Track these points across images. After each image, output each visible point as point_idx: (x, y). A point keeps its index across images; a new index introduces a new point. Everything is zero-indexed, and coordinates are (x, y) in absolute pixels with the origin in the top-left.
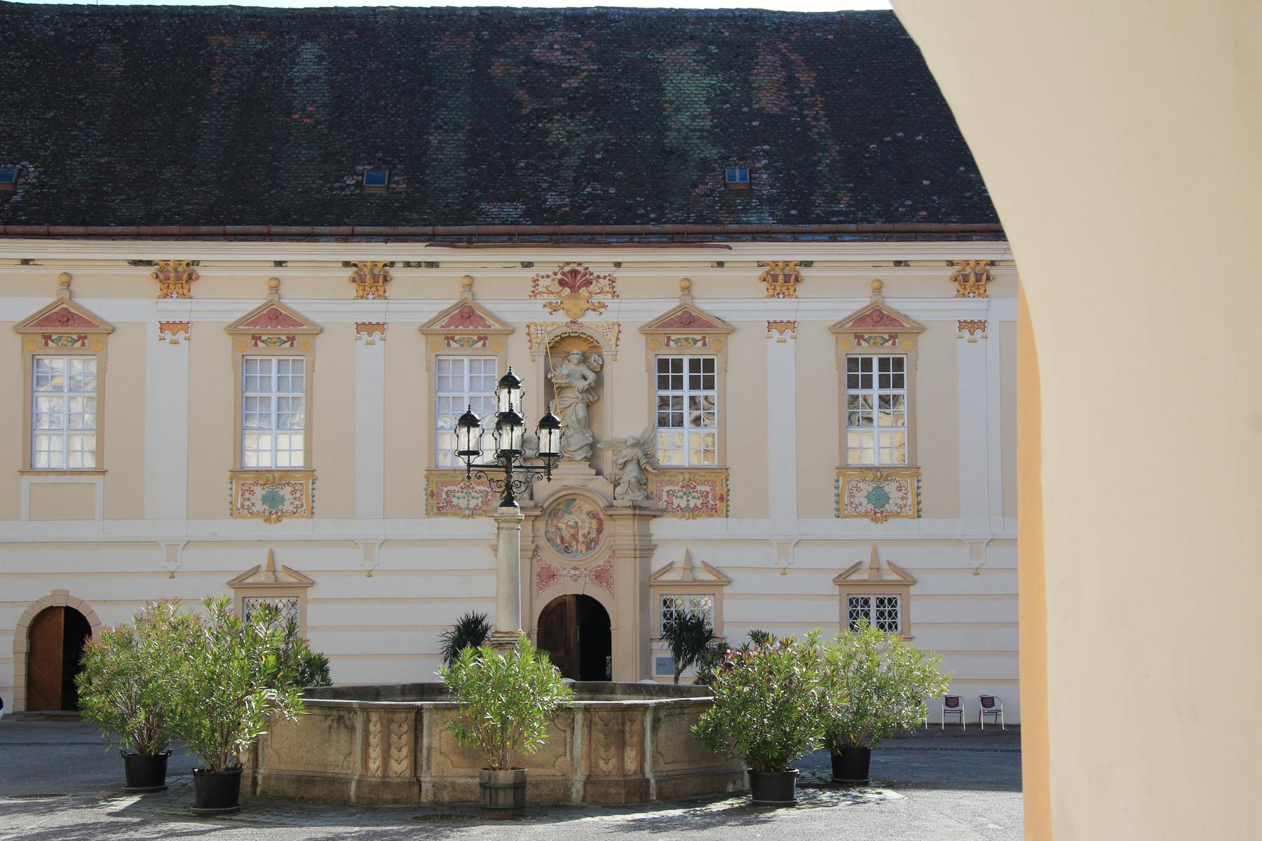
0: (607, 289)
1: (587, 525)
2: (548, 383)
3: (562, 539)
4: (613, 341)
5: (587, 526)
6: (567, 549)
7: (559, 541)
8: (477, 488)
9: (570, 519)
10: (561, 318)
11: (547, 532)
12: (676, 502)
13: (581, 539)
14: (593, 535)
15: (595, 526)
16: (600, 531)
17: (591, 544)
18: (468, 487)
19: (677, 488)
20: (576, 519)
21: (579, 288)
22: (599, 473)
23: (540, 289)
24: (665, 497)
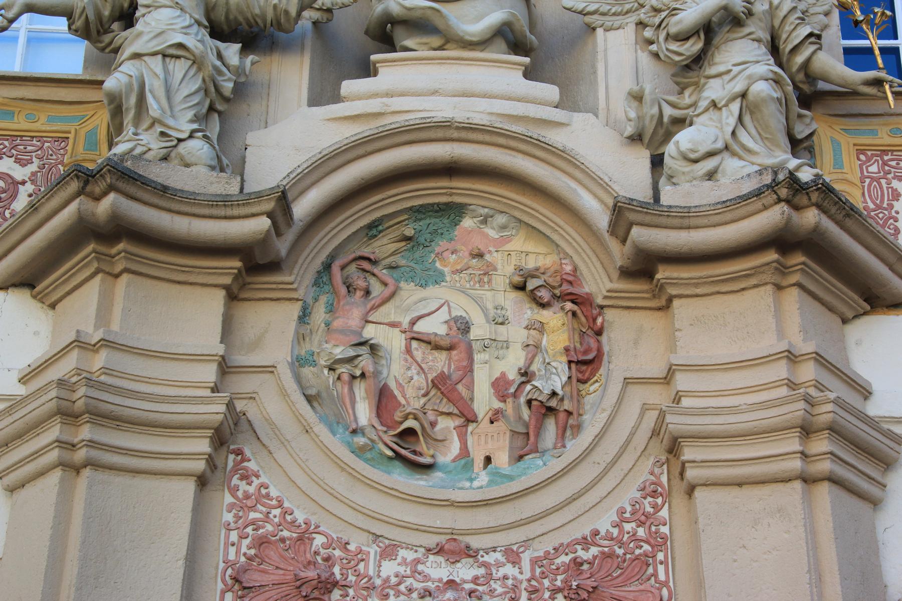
1: (516, 333)
3: (383, 400)
5: (516, 343)
6: (407, 448)
7: (364, 413)
9: (432, 305)
11: (299, 362)
13: (483, 400)
14: (554, 378)
16: (585, 364)
20: (462, 306)
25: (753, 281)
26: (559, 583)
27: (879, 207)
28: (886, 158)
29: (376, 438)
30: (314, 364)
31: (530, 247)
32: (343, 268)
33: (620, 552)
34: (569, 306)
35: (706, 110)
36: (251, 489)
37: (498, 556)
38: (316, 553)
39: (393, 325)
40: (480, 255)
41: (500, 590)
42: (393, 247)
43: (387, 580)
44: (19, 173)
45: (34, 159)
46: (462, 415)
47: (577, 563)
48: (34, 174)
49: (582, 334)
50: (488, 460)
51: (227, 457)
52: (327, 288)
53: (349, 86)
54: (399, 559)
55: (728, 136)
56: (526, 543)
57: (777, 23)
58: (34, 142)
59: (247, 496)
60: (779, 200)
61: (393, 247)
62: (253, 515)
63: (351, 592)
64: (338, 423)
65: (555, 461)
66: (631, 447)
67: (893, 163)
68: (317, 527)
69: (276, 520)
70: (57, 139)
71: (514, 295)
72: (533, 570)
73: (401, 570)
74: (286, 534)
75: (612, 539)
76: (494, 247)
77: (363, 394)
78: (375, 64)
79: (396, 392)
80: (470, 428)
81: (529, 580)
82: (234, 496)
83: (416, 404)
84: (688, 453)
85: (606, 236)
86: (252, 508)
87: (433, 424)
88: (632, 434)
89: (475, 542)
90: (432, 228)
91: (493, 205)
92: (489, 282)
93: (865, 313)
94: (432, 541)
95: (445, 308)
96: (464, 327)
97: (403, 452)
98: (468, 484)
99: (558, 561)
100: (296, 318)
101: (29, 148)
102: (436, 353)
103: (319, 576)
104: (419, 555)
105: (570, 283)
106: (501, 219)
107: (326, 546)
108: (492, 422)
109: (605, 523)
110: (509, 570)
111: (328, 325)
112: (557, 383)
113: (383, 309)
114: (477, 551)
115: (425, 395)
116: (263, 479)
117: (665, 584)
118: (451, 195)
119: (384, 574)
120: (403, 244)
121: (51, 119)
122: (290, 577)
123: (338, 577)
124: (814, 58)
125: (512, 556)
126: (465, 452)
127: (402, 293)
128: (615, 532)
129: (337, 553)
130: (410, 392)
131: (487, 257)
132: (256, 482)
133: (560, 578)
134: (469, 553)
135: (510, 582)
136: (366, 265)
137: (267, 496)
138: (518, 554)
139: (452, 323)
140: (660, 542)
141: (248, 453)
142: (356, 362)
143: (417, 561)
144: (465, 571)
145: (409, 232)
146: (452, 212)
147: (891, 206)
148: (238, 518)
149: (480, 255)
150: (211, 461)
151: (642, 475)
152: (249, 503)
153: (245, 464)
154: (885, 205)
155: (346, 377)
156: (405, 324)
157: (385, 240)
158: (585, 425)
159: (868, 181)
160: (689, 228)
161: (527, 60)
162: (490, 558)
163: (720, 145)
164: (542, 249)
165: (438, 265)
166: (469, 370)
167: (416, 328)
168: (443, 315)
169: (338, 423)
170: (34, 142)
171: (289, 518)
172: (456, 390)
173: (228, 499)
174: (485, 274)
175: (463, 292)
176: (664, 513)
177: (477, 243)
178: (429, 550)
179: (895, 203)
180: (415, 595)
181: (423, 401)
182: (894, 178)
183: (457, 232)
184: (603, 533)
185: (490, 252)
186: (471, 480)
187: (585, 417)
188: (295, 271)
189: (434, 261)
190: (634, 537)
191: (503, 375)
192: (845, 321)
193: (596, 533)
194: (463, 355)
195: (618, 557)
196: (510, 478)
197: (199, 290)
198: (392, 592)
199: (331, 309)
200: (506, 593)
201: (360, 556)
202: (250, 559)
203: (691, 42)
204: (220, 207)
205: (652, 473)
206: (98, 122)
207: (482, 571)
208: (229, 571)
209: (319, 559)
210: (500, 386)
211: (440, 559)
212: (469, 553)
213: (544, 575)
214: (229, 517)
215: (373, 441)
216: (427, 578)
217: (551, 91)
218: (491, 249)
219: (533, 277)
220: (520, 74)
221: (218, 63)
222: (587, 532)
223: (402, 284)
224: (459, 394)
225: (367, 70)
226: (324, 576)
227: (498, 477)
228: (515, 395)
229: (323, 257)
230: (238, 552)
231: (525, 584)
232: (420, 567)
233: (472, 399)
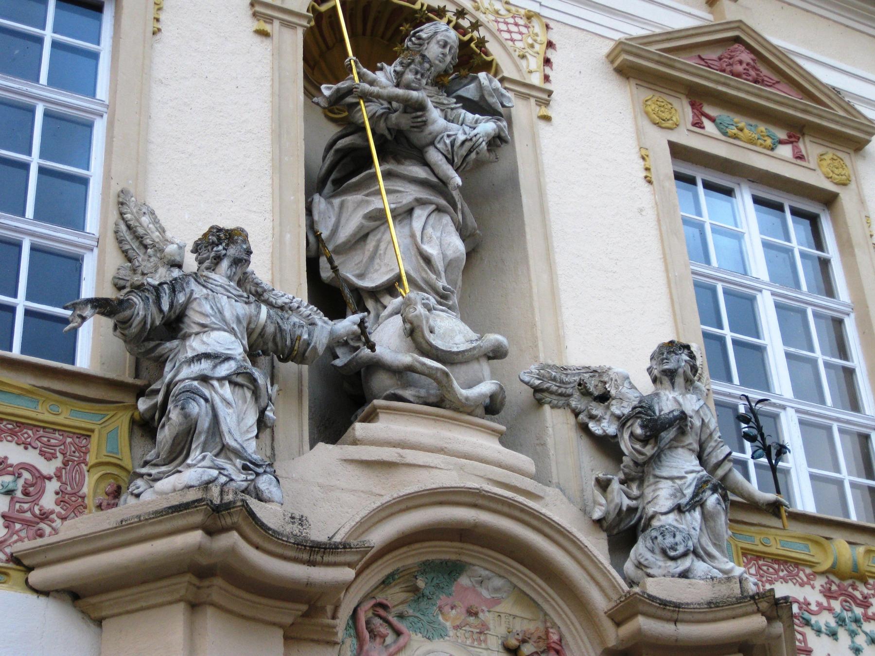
28: (761, 562)
31: (517, 611)
32: (366, 612)
40: (476, 614)
44: (48, 468)
45: (58, 454)
48: (59, 470)
53: (359, 428)
57: (703, 438)
60: (759, 611)
61: (403, 596)
67: (765, 568)
91: (497, 570)
92: (485, 641)
101: (53, 441)
106: (498, 582)
131: (481, 615)
136: (382, 612)
146: (452, 570)
149: (476, 614)
157: (397, 589)
174: (480, 633)
177: (471, 600)
185: (483, 611)
218: (484, 608)
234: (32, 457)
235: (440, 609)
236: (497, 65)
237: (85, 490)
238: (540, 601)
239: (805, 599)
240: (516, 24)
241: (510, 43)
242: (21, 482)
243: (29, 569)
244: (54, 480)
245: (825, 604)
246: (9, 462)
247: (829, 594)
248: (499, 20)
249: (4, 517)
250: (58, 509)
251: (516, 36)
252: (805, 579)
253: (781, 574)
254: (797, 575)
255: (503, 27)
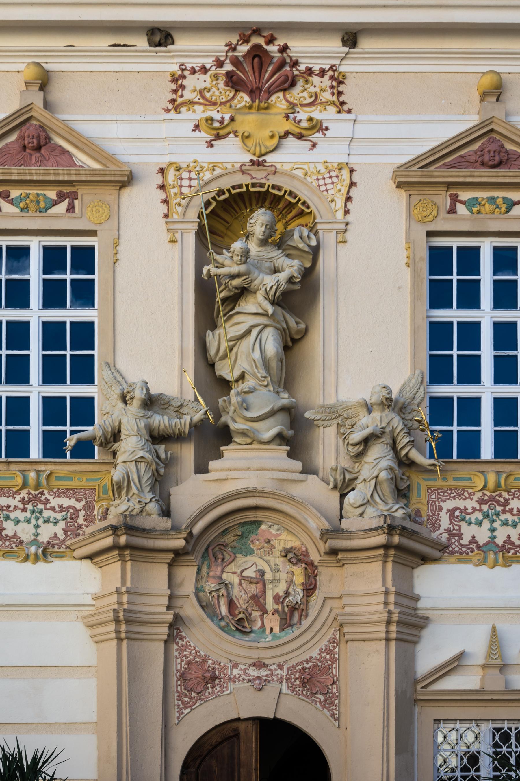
0: (327, 96)
1: (283, 576)
2: (205, 289)
3: (231, 604)
4: (340, 202)
5: (283, 580)
6: (241, 626)
8: (55, 502)
9: (249, 564)
10: (231, 153)
11: (198, 591)
12: (468, 532)
15: (299, 578)
16: (310, 589)
17: (291, 614)
18: (35, 499)
19: (470, 504)
20: (262, 565)
21: (270, 93)
22: (308, 470)
23: (188, 95)
24: (445, 522)
25: (375, 559)
26: (297, 676)
27: (434, 515)
28: (439, 491)
29: (229, 621)
30: (204, 591)
31: (289, 538)
32: (213, 550)
33: (320, 664)
34: (304, 565)
35: (362, 482)
36: (184, 643)
37: (275, 667)
38: (209, 667)
39: (234, 573)
41: (276, 679)
42: (233, 539)
43: (235, 676)
44: (79, 506)
45: (83, 499)
46: (261, 611)
47: (304, 669)
48: (84, 506)
49: (309, 577)
50: (271, 629)
51: (174, 631)
52: (207, 558)
53: (213, 464)
54: (239, 668)
55: (369, 497)
56: (286, 662)
58: (82, 491)
59: (183, 646)
62: (185, 653)
63: (222, 680)
64: (214, 616)
65: (297, 631)
66: (326, 624)
67: (442, 494)
68: (209, 657)
69: (194, 655)
70: (91, 489)
71: (282, 559)
72: (288, 672)
73: (240, 672)
74: (198, 660)
75: (317, 660)
76: (274, 537)
77: (223, 602)
78: (222, 451)
79: (236, 602)
80: (265, 615)
81: (286, 676)
82: (178, 645)
83: (244, 607)
84: (346, 629)
85: (319, 540)
86: (185, 650)
87: (250, 615)
88: (326, 620)
89: (267, 662)
90: (248, 530)
93: (422, 564)
94: (251, 661)
95: (254, 565)
96: (262, 573)
97: (240, 627)
98: (264, 640)
99: (297, 668)
100: (195, 573)
101: (81, 494)
102: (251, 585)
103: (211, 675)
104: (246, 667)
105: (304, 555)
106: (277, 527)
107: (213, 664)
108: (273, 615)
109: (314, 653)
110: (279, 672)
111: (208, 574)
112: (298, 598)
113: (229, 566)
114: (268, 665)
115: (248, 602)
116: (188, 639)
117: (336, 675)
118: (256, 517)
119: (234, 674)
120: (237, 537)
121: (88, 480)
122: (200, 676)
123: (217, 675)
124: (410, 452)
125: (280, 667)
126: (263, 625)
127: (237, 559)
128: (318, 657)
129: (217, 666)
130: (241, 602)
131: (271, 542)
132: (185, 640)
133: (297, 674)
134: (265, 665)
135: (279, 676)
136: (222, 547)
137: (190, 645)
138: (282, 666)
139: (257, 572)
140: (334, 660)
141: (181, 630)
142: (220, 590)
143: (246, 669)
144: (263, 673)
145: (239, 533)
147: (439, 514)
148: (180, 654)
149: (269, 542)
150: (169, 635)
151: (330, 635)
152: (183, 648)
153: (181, 633)
154: (436, 514)
155: (216, 597)
156: (239, 573)
157: (229, 536)
158: (309, 614)
159: (430, 502)
160: (351, 539)
161: (288, 448)
162: (272, 668)
163: (365, 501)
164: (294, 539)
165: (251, 546)
166: (264, 592)
167: (244, 574)
168: (254, 568)
169: (214, 616)
170: (82, 491)
171: (198, 654)
172: (259, 601)
173: (176, 647)
175: (262, 558)
176: (337, 650)
178: (250, 665)
179: (440, 513)
180: (245, 681)
181: (246, 605)
182: (441, 501)
183: (259, 531)
184: (314, 657)
185: (272, 540)
186: (265, 638)
187: (309, 611)
188: (194, 555)
189: (250, 545)
190: (325, 659)
191: (278, 594)
192: (413, 568)
193: (311, 658)
194: (262, 586)
195: (319, 666)
196: (280, 638)
197: (158, 564)
198: (237, 681)
199: (209, 567)
200: (278, 680)
201: (225, 668)
202: (186, 669)
203: (358, 446)
204: (166, 533)
205: (333, 634)
206: (107, 480)
207: (269, 672)
208: (178, 673)
209: (210, 669)
210: (276, 598)
211: (254, 668)
212: (265, 665)
213: (292, 673)
214: (176, 654)
215: (227, 623)
216: (249, 675)
217: (298, 465)
219: (290, 552)
220: (286, 454)
221: (157, 460)
222: (308, 657)
223: (237, 555)
224: (261, 602)
225: (219, 456)
226: (213, 675)
227: (275, 637)
228: (282, 603)
229: (205, 547)
230: (181, 667)
231: (285, 677)
232: (247, 671)
233: (265, 604)
234: (72, 502)
235: (252, 541)
236: (314, 213)
237: (95, 513)
238: (296, 533)
239: (465, 507)
240: (331, 177)
241: (325, 193)
242: (69, 514)
243: (74, 550)
244: (82, 511)
245: (478, 508)
246: (64, 506)
247: (481, 502)
248: (319, 178)
249: (63, 530)
250: (85, 523)
251: (329, 187)
252: (467, 496)
253: (452, 495)
254: (463, 494)
255: (321, 182)
